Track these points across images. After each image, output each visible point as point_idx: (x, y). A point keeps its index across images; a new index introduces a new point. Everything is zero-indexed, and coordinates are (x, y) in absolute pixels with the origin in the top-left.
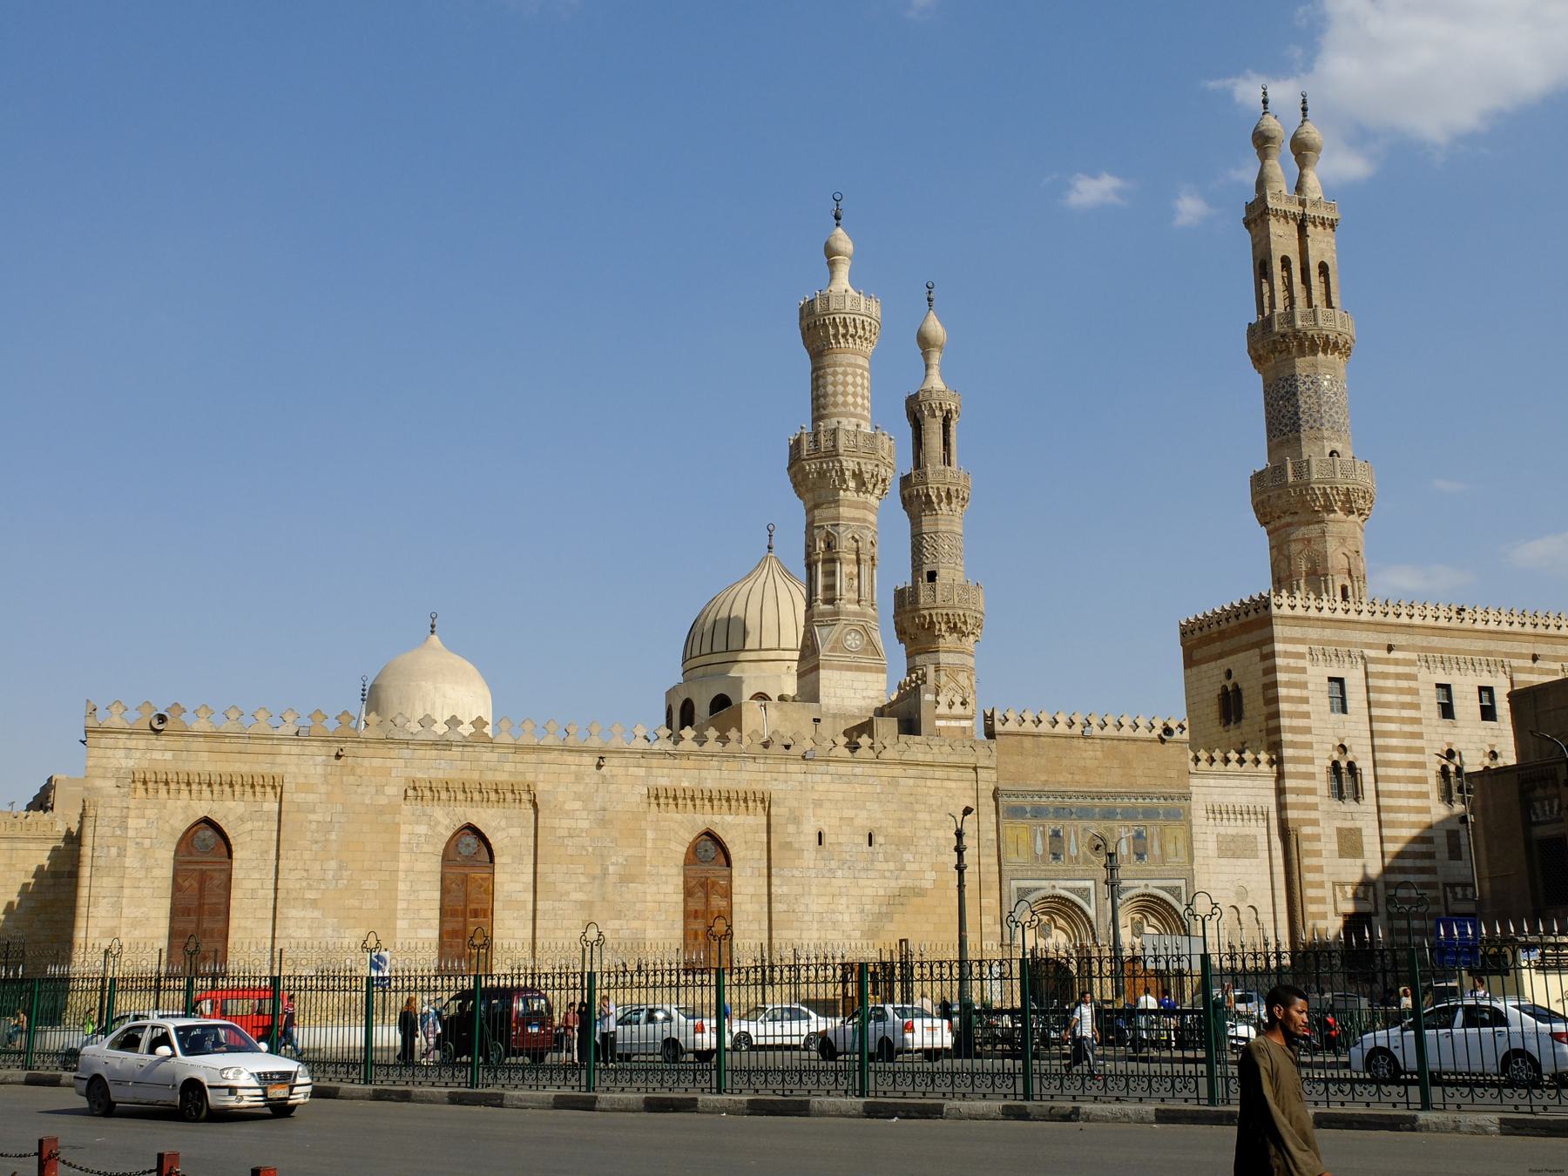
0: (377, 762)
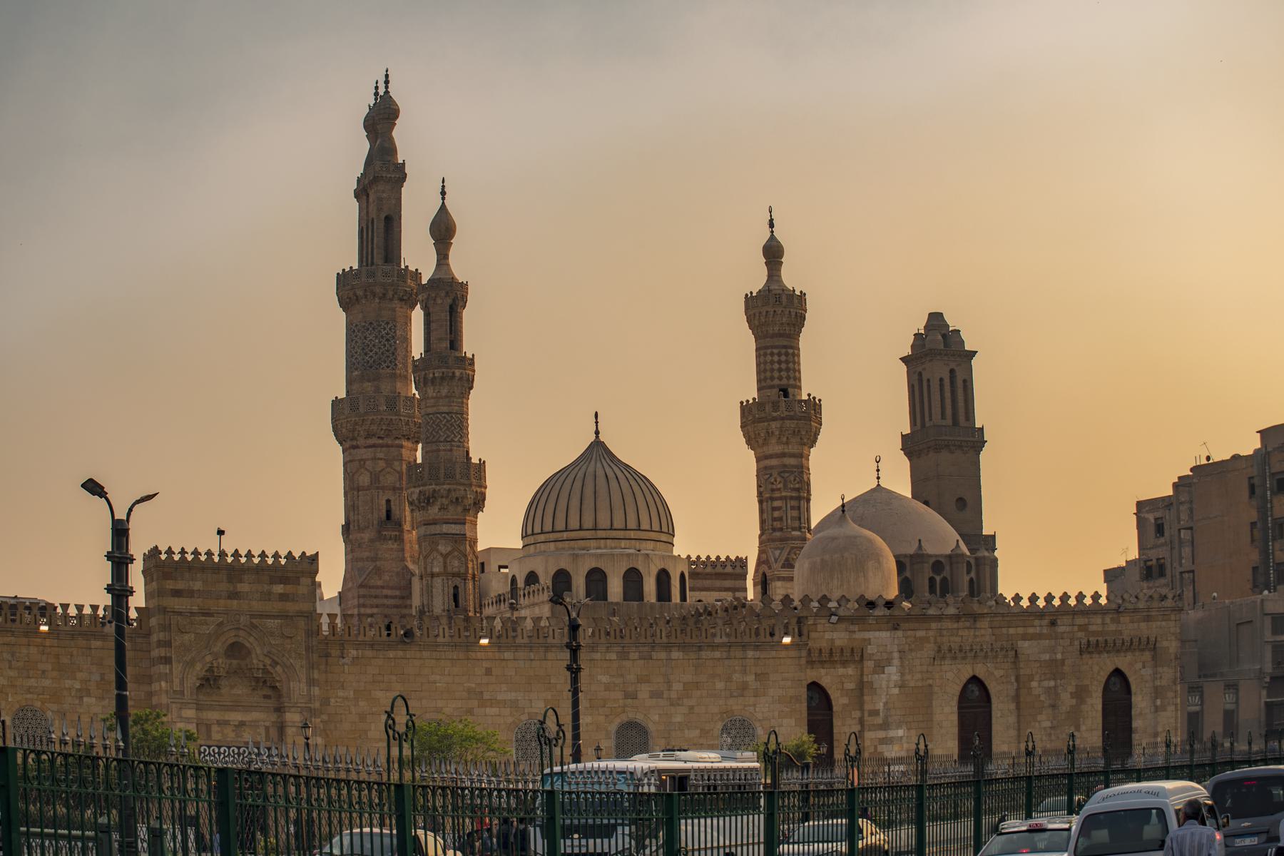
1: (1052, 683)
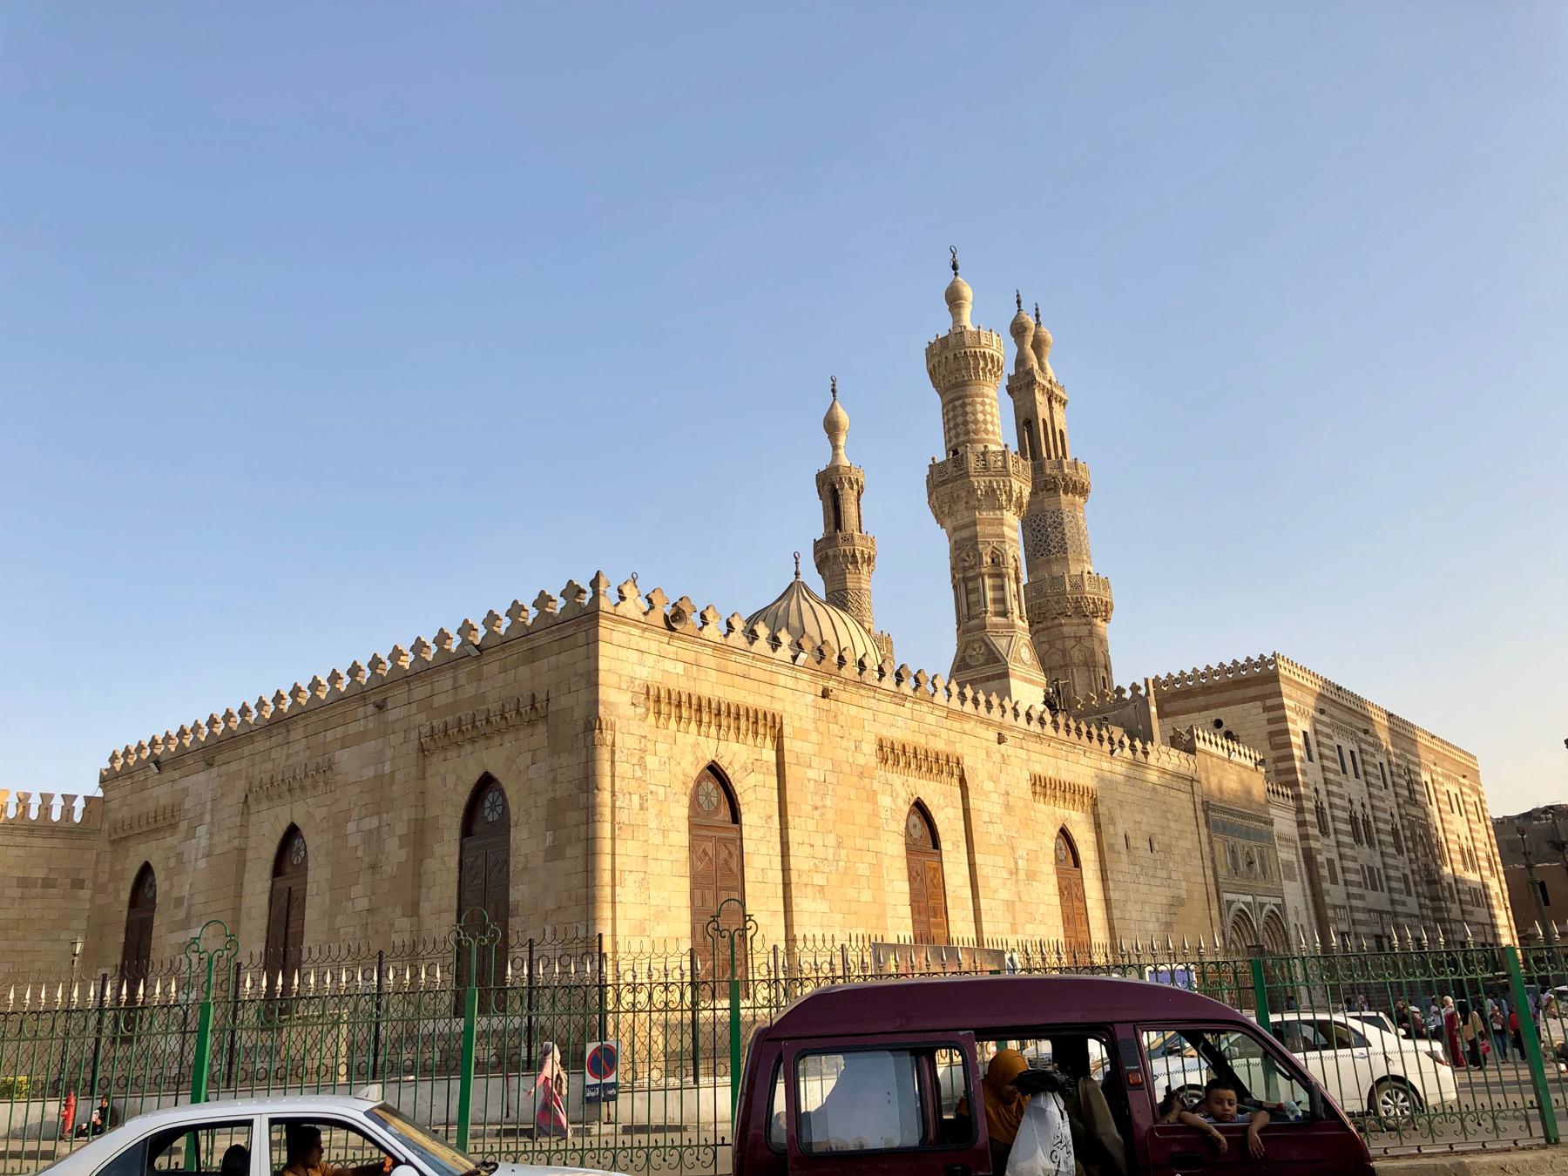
0: (853, 710)
1: (373, 822)
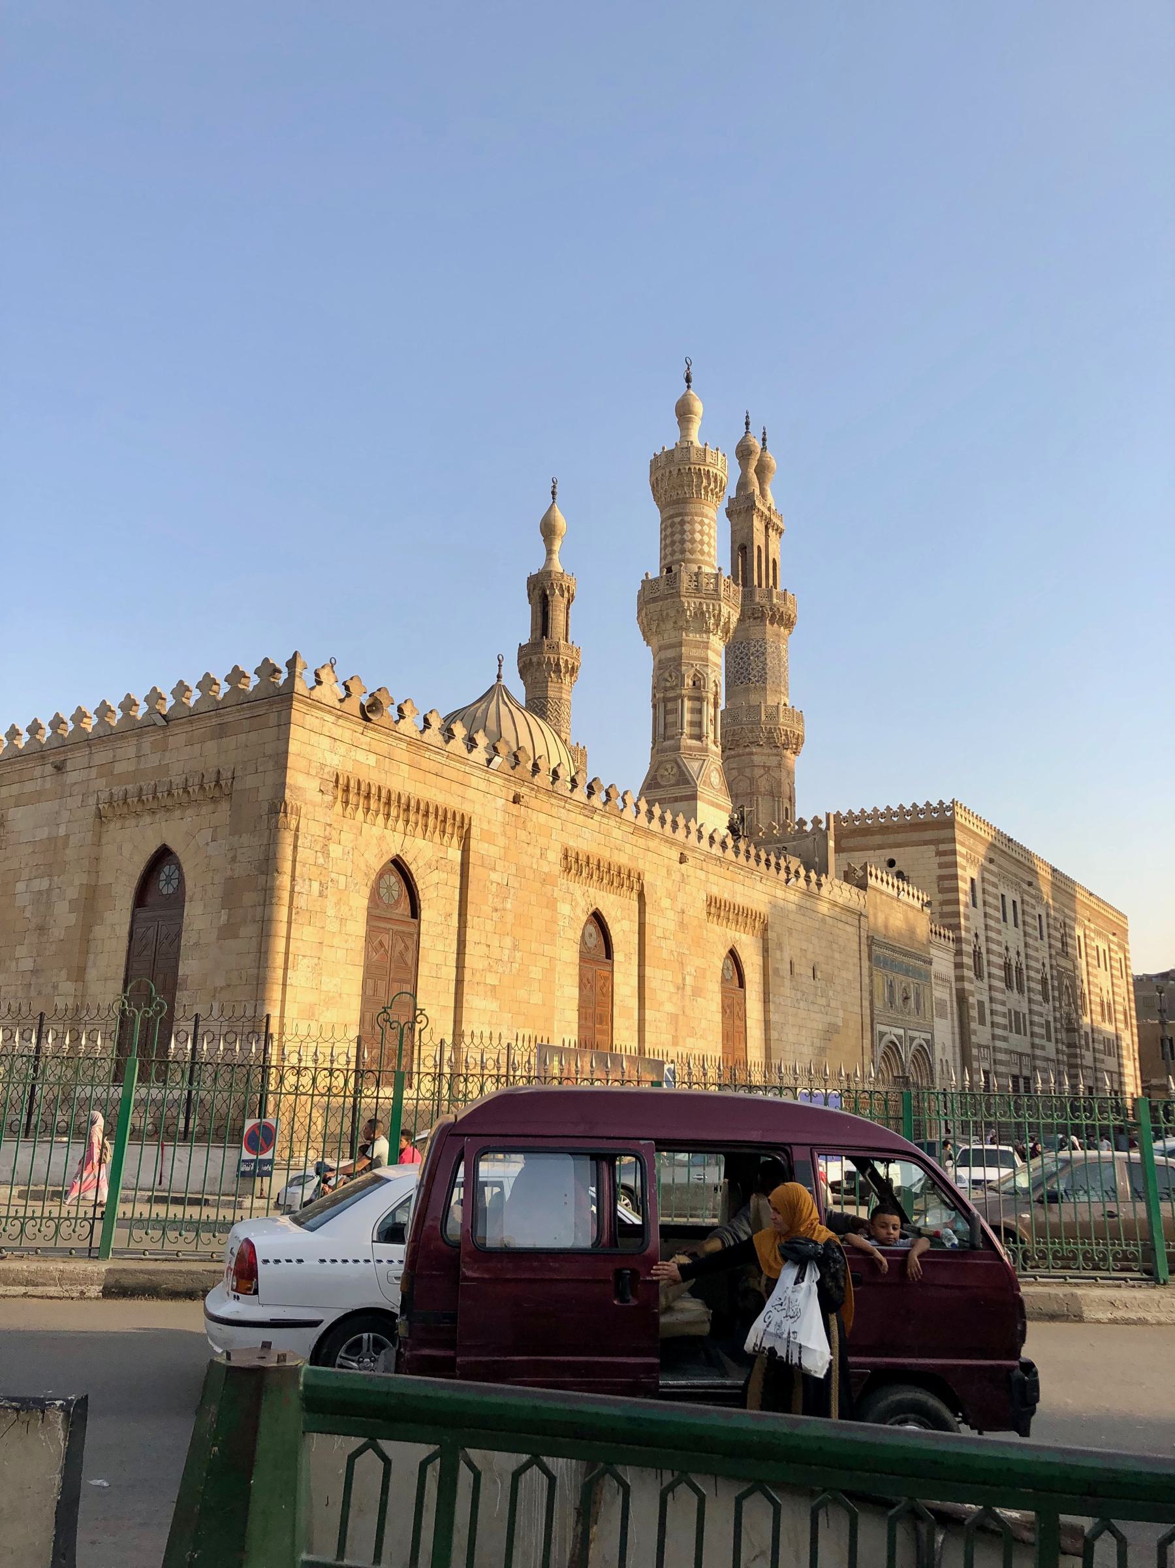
0: (542, 818)
1: (44, 884)
